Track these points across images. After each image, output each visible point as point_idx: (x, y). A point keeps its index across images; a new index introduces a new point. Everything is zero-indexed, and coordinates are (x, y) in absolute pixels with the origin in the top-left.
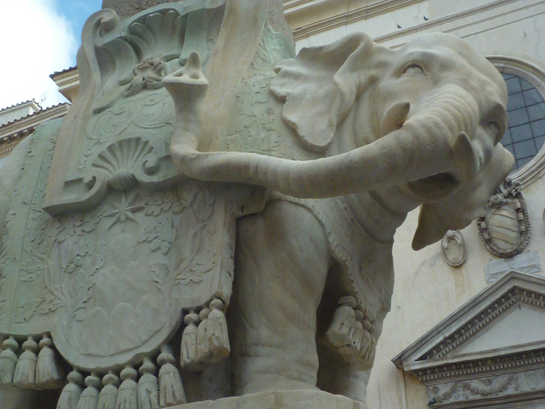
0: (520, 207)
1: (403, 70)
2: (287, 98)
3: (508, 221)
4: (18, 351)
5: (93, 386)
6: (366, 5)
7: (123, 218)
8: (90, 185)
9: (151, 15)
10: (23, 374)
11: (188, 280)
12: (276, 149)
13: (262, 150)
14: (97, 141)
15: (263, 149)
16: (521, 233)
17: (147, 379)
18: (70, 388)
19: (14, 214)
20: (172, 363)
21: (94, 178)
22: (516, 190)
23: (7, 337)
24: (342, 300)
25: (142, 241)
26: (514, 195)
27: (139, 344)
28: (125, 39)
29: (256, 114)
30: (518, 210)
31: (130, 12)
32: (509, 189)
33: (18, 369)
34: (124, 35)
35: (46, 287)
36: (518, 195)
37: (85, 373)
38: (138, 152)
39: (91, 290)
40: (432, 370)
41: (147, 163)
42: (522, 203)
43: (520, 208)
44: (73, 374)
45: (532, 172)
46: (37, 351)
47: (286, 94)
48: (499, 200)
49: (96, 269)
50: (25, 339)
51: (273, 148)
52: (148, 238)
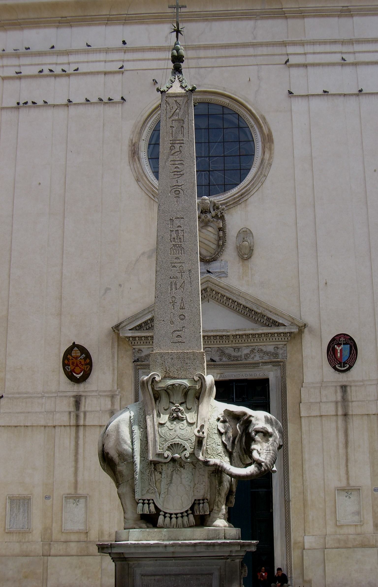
0: (222, 226)
1: (257, 432)
2: (224, 433)
3: (212, 235)
5: (169, 517)
6: (126, 13)
7: (177, 469)
8: (167, 458)
9: (176, 385)
14: (165, 439)
16: (218, 245)
17: (185, 519)
20: (191, 513)
21: (168, 455)
22: (221, 213)
23: (140, 499)
26: (219, 216)
28: (165, 390)
29: (215, 438)
30: (220, 229)
32: (216, 211)
33: (144, 509)
34: (165, 389)
35: (150, 485)
36: (222, 218)
37: (166, 513)
38: (181, 448)
40: (140, 338)
41: (186, 455)
42: (224, 224)
43: (222, 228)
44: (162, 513)
45: (234, 199)
46: (149, 504)
48: (208, 218)
50: (145, 500)
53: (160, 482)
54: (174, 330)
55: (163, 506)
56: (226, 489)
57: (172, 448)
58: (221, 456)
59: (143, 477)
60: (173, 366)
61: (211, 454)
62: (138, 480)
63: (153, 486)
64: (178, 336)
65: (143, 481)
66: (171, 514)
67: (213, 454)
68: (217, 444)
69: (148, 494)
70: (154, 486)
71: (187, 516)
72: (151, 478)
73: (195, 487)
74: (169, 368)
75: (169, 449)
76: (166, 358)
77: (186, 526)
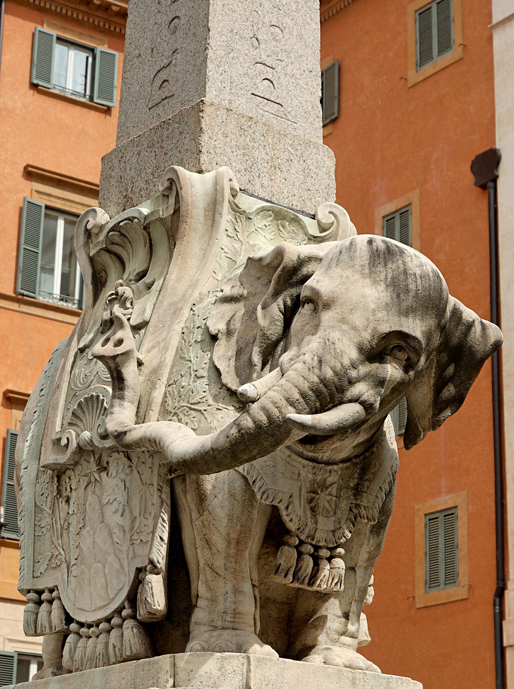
2: (220, 336)
4: (39, 603)
7: (93, 480)
10: (42, 625)
11: (139, 540)
12: (204, 400)
13: (191, 404)
15: (192, 402)
18: (71, 638)
19: (27, 468)
23: (29, 591)
24: (286, 538)
25: (105, 503)
27: (109, 601)
31: (120, 201)
37: (81, 625)
39: (78, 548)
44: (73, 626)
47: (217, 332)
49: (80, 528)
51: (200, 400)
52: (110, 500)
53: (68, 526)
54: (157, 68)
55: (74, 605)
56: (225, 521)
57: (81, 416)
58: (200, 411)
59: (39, 521)
60: (139, 175)
61: (173, 411)
62: (25, 533)
63: (57, 545)
64: (163, 83)
65: (40, 534)
66: (90, 626)
67: (179, 408)
68: (193, 376)
69: (51, 572)
70: (59, 544)
71: (121, 626)
72: (54, 519)
73: (135, 529)
74: (132, 185)
75: (75, 421)
76: (127, 158)
77: (112, 660)
